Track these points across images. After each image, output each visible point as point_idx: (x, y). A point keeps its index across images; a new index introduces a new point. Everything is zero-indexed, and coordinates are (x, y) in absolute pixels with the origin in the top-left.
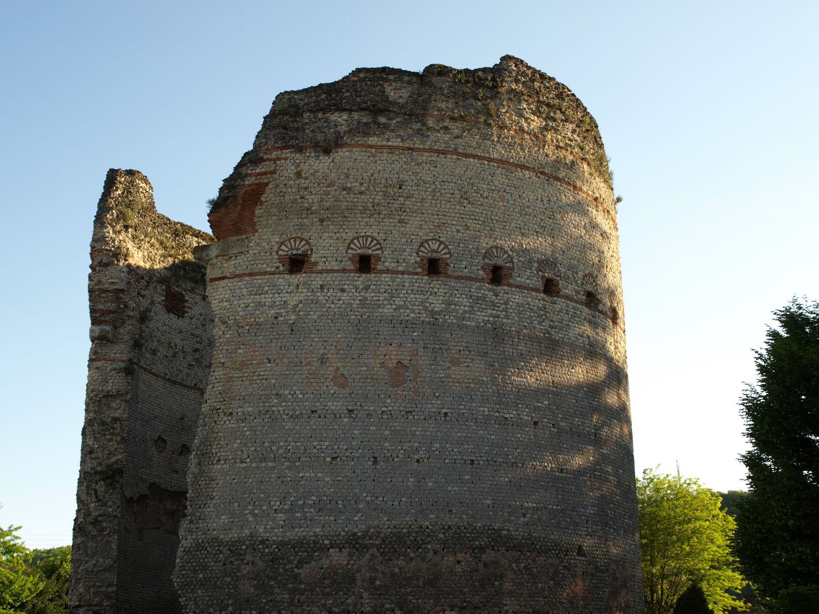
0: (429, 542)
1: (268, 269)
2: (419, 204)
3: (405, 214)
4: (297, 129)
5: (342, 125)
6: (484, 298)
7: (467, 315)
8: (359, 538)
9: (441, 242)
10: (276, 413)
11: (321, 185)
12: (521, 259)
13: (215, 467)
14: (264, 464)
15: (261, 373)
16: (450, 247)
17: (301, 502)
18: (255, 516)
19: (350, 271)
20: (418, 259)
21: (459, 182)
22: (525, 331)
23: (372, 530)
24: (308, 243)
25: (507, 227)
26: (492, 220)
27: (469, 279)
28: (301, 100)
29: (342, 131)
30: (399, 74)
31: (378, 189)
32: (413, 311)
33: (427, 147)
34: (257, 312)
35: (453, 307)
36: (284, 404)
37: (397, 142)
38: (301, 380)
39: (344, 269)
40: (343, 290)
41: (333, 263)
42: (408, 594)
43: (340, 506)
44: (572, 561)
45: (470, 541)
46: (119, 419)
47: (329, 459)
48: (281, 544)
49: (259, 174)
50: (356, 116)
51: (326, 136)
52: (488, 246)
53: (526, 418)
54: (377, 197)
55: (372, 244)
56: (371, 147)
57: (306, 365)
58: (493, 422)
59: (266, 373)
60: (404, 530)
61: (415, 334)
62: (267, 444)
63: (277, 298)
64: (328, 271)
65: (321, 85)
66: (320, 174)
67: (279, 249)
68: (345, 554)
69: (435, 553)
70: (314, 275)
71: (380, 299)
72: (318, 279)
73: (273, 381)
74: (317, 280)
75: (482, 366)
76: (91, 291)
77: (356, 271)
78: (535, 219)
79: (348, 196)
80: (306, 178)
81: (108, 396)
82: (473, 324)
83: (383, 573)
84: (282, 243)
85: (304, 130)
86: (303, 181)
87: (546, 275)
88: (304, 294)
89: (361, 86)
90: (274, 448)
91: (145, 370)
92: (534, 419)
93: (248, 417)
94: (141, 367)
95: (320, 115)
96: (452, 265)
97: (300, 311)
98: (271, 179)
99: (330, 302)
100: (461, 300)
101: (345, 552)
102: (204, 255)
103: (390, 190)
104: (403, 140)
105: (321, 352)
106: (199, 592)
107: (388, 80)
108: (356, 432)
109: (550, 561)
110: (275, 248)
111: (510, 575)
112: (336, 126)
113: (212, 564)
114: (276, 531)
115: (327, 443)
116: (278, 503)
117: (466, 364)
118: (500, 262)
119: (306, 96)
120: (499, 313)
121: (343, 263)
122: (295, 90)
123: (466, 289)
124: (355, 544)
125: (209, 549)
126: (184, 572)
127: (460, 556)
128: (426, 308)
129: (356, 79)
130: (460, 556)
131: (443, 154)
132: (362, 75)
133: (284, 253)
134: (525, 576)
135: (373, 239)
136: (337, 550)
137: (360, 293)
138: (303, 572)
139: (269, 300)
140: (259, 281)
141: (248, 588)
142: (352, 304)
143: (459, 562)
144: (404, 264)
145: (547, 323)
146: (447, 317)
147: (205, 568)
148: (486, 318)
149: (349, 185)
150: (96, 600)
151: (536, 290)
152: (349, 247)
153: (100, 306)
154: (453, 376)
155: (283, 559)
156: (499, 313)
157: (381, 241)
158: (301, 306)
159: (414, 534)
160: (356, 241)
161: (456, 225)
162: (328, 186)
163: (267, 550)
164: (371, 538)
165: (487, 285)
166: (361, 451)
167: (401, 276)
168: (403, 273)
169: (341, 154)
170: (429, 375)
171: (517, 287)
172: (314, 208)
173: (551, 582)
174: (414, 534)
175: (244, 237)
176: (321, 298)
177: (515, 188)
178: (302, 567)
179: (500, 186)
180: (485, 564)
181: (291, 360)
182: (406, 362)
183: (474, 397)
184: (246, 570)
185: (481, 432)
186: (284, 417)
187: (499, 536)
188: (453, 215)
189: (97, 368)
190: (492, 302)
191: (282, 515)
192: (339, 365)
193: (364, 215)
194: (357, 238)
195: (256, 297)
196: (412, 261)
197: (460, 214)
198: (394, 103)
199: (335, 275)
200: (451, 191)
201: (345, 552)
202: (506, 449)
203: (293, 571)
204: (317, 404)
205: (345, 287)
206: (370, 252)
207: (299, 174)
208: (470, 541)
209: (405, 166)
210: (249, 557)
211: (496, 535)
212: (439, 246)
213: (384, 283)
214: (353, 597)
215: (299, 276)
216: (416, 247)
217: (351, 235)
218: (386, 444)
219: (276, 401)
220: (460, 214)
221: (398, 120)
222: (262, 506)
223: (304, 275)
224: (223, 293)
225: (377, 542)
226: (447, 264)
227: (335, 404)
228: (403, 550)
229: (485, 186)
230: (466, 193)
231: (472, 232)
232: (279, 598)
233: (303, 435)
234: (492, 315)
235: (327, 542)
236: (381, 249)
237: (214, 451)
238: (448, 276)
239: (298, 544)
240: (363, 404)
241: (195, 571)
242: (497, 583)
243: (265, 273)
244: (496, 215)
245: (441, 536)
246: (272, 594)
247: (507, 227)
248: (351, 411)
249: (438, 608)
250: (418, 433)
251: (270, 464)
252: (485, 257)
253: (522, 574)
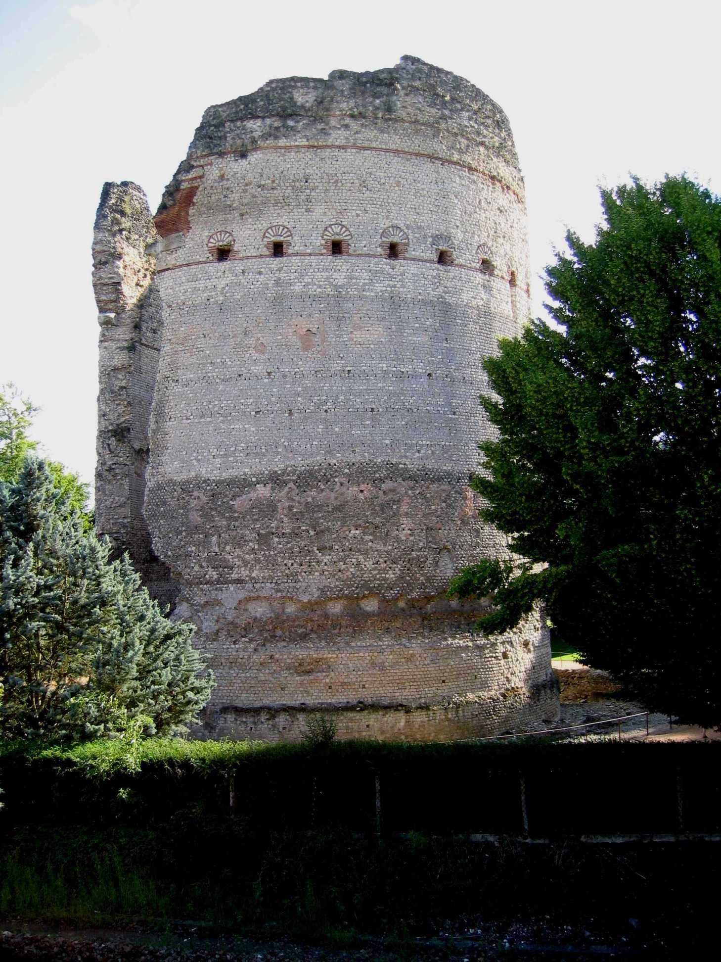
0: (336, 477)
1: (201, 260)
2: (323, 195)
3: (311, 204)
4: (220, 138)
5: (256, 131)
6: (382, 272)
7: (367, 287)
8: (279, 475)
9: (343, 226)
10: (211, 378)
11: (240, 185)
12: (416, 235)
13: (168, 423)
14: (203, 420)
15: (199, 346)
16: (351, 230)
17: (233, 449)
18: (198, 460)
19: (266, 256)
20: (323, 242)
21: (359, 172)
22: (420, 297)
23: (289, 469)
24: (231, 235)
25: (403, 209)
26: (389, 203)
27: (368, 255)
28: (224, 111)
29: (256, 136)
30: (305, 81)
31: (287, 184)
32: (320, 286)
34: (194, 296)
35: (354, 281)
36: (217, 370)
37: (304, 142)
38: (229, 350)
39: (261, 255)
40: (260, 273)
41: (252, 251)
42: (320, 518)
43: (264, 450)
44: (463, 487)
45: (371, 474)
46: (125, 388)
47: (253, 413)
48: (219, 483)
49: (192, 179)
50: (268, 121)
51: (243, 142)
52: (385, 226)
53: (420, 371)
54: (287, 191)
55: (284, 232)
56: (280, 148)
57: (233, 337)
58: (391, 375)
59: (202, 346)
60: (316, 468)
61: (322, 306)
62: (205, 404)
63: (209, 284)
64: (248, 258)
65: (240, 98)
66: (239, 175)
67: (209, 242)
68: (268, 488)
69: (342, 485)
70: (237, 262)
71: (292, 278)
73: (208, 352)
74: (239, 266)
75: (380, 329)
76: (95, 285)
77: (270, 256)
78: (429, 199)
79: (262, 192)
80: (228, 180)
81: (115, 369)
82: (372, 294)
83: (299, 502)
84: (211, 237)
85: (226, 138)
87: (440, 247)
88: (230, 278)
89: (273, 95)
90: (210, 406)
91: (147, 346)
92: (428, 372)
93: (190, 382)
94: (142, 344)
95: (239, 123)
96: (353, 245)
97: (227, 293)
98: (200, 183)
99: (250, 284)
100: (361, 274)
101: (269, 486)
102: (153, 250)
103: (297, 184)
104: (308, 140)
105: (245, 325)
106: (161, 521)
107: (295, 87)
108: (274, 390)
109: (442, 487)
110: (206, 242)
111: (407, 500)
112: (252, 132)
113: (170, 500)
114: (215, 472)
115: (251, 400)
116: (216, 450)
117: (367, 329)
118: (396, 240)
119: (228, 108)
120: (396, 283)
121: (260, 250)
122: (220, 104)
123: (366, 265)
124: (276, 480)
125: (166, 488)
126: (150, 507)
127: (362, 487)
128: (330, 284)
129: (269, 89)
130: (362, 487)
131: (343, 149)
132: (274, 85)
134: (420, 501)
135: (284, 227)
136: (262, 485)
137: (274, 274)
138: (236, 503)
139: (202, 285)
140: (194, 270)
141: (196, 518)
142: (268, 284)
143: (362, 491)
144: (311, 247)
145: (441, 289)
146: (349, 290)
147: (164, 503)
148: (384, 289)
149: (263, 183)
150: (115, 529)
151: (431, 261)
152: (264, 236)
153: (103, 298)
154: (355, 340)
155: (221, 494)
156: (396, 283)
157: (291, 229)
158: (227, 288)
159: (324, 471)
160: (270, 231)
161: (356, 210)
162: (246, 185)
163: (208, 488)
164: (288, 475)
165: (384, 260)
166: (278, 405)
167: (308, 258)
168: (310, 255)
169: (255, 157)
170: (334, 339)
171: (413, 259)
172: (235, 205)
173: (444, 504)
174: (324, 471)
175: (181, 233)
177: (410, 173)
178: (235, 500)
179: (396, 173)
180: (384, 492)
181: (221, 334)
182: (314, 330)
183: (373, 356)
184: (193, 503)
185: (380, 385)
186: (218, 380)
187: (397, 469)
188: (353, 201)
189: (105, 348)
190: (389, 274)
191: (219, 460)
192: (259, 335)
193: (276, 208)
194: (271, 228)
195: (193, 283)
196: (319, 244)
197: (360, 200)
198: (302, 107)
199: (254, 260)
200: (352, 181)
201: (269, 486)
202: (402, 398)
203: (228, 503)
204: (243, 369)
205: (262, 270)
206: (282, 239)
208: (371, 474)
209: (310, 162)
210: (196, 494)
211: (394, 468)
212: (341, 229)
213: (294, 265)
214: (276, 522)
215: (225, 263)
216: (321, 231)
217: (266, 225)
218: (299, 399)
219: (210, 368)
220: (360, 200)
221: (305, 122)
222: (203, 453)
223: (229, 262)
224: (168, 281)
225: (294, 478)
226: (349, 245)
227: (257, 368)
228: (315, 483)
229: (382, 174)
230: (364, 182)
231: (371, 216)
232: (219, 524)
233: (232, 395)
234: (389, 285)
235: (254, 479)
236: (291, 235)
237: (166, 411)
238: (350, 255)
239: (231, 483)
240: (280, 367)
241: (158, 505)
242: (395, 507)
243: (199, 263)
244: (393, 199)
245: (346, 471)
246: (214, 521)
247: (403, 209)
248: (269, 374)
249: (345, 528)
250: (325, 388)
251: (208, 419)
252: (382, 235)
253: (417, 498)
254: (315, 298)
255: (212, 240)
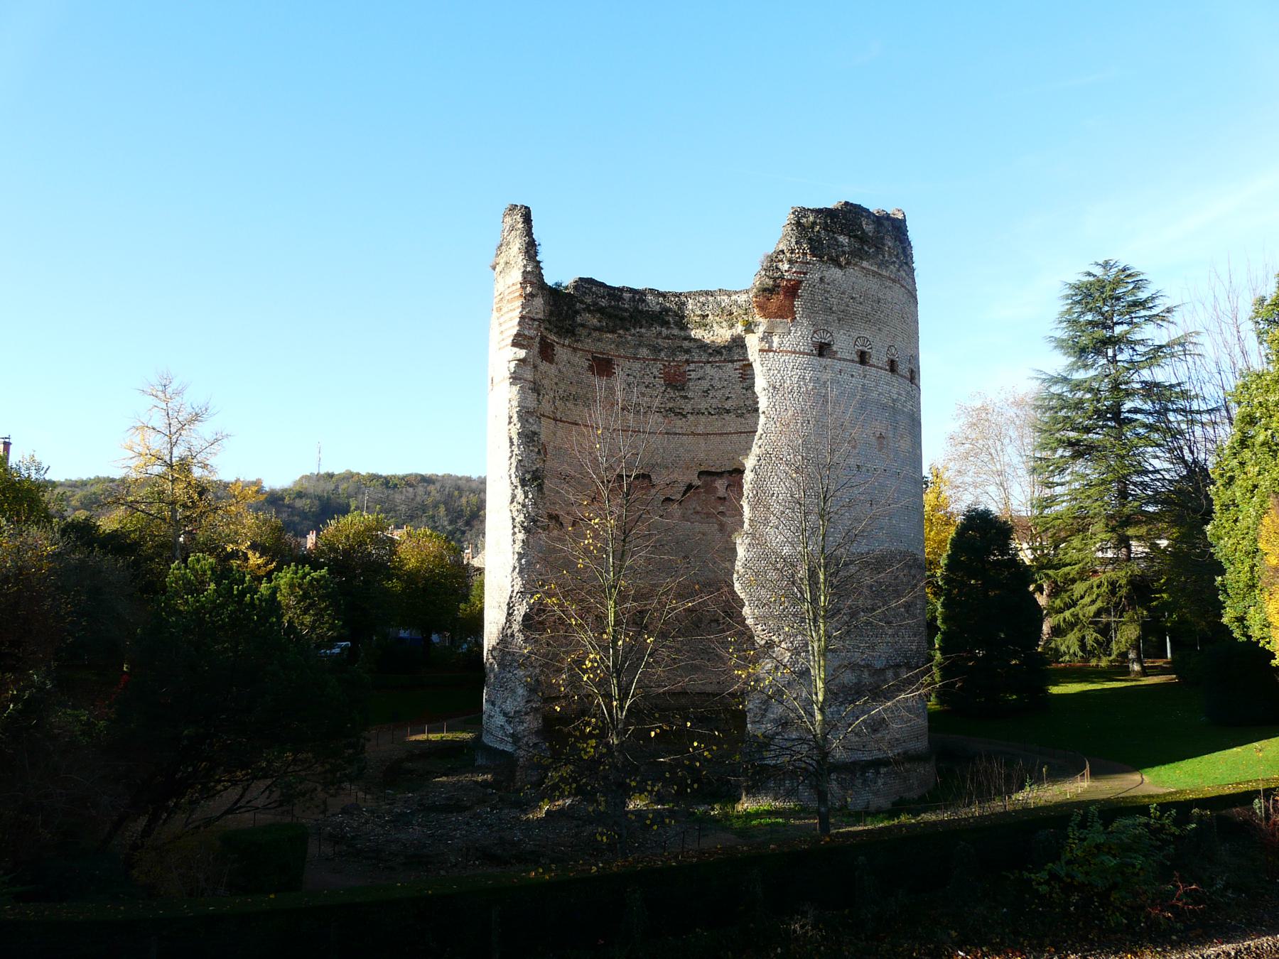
24: (831, 335)
33: (888, 275)
40: (852, 376)
41: (847, 354)
64: (845, 360)
72: (838, 364)
74: (838, 365)
86: (826, 286)
133: (817, 340)
152: (855, 344)
176: (840, 379)
199: (848, 363)
205: (854, 373)
207: (821, 279)
217: (855, 335)
223: (829, 360)
254: (884, 407)
255: (815, 335)
